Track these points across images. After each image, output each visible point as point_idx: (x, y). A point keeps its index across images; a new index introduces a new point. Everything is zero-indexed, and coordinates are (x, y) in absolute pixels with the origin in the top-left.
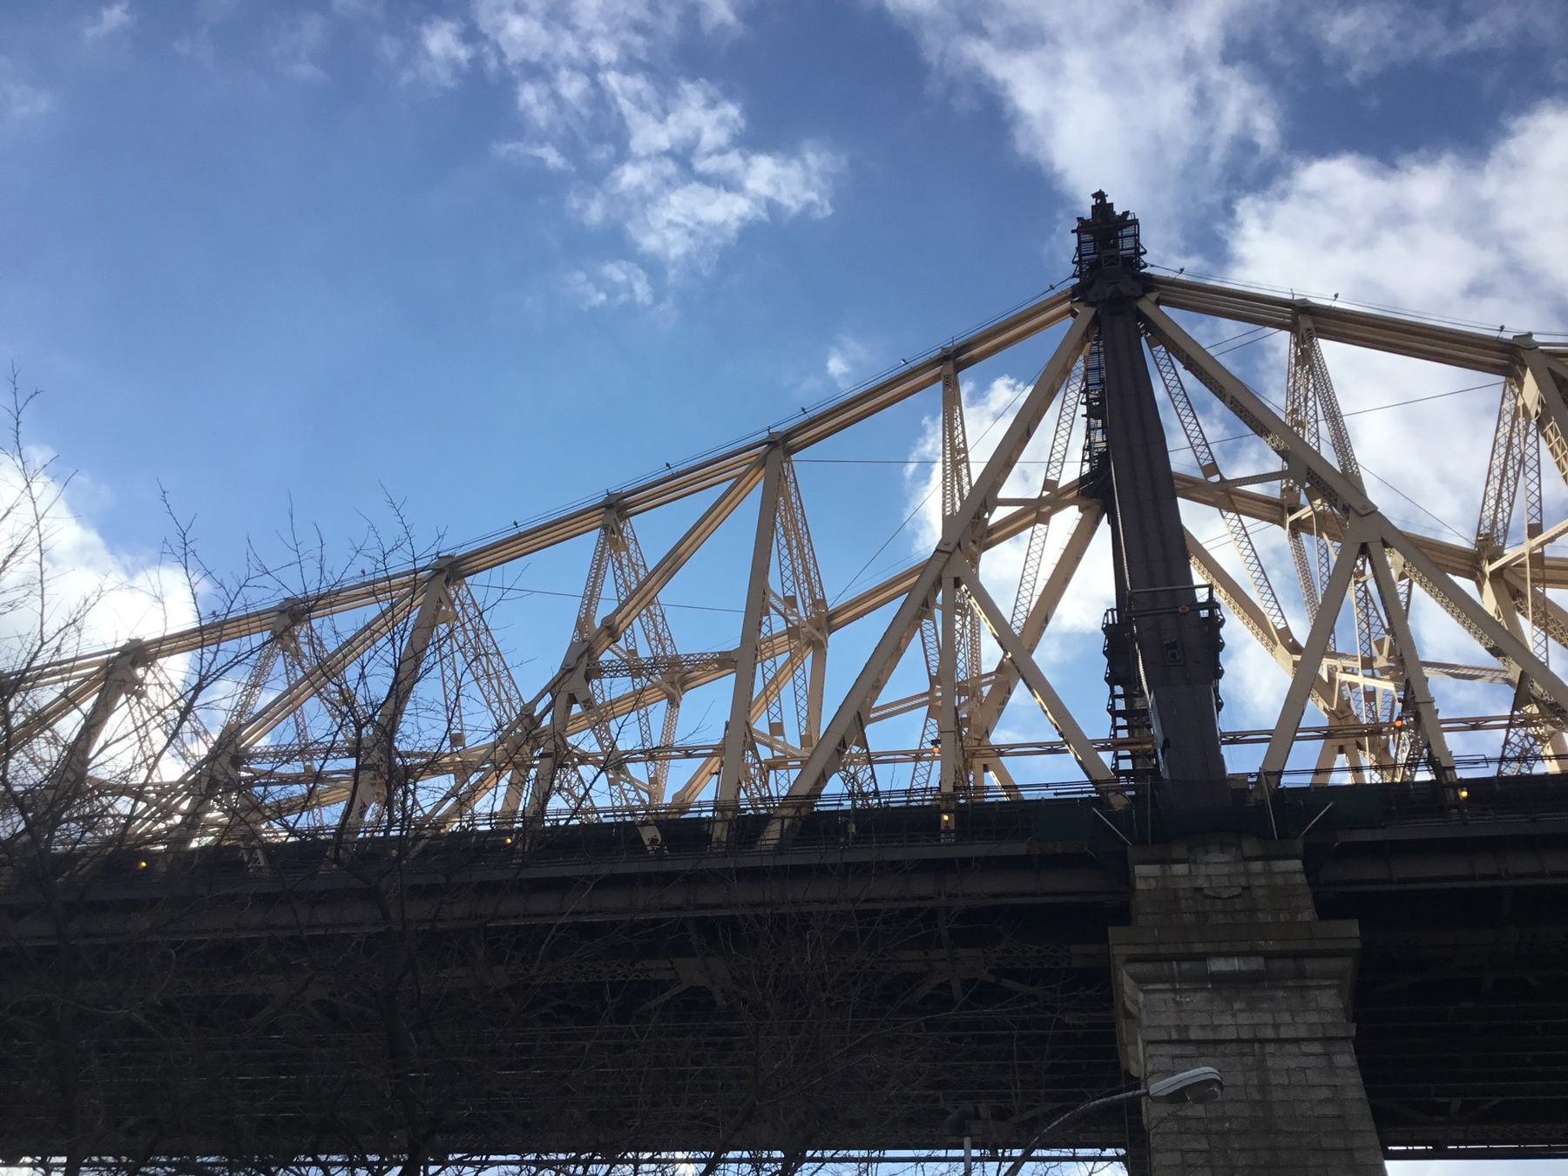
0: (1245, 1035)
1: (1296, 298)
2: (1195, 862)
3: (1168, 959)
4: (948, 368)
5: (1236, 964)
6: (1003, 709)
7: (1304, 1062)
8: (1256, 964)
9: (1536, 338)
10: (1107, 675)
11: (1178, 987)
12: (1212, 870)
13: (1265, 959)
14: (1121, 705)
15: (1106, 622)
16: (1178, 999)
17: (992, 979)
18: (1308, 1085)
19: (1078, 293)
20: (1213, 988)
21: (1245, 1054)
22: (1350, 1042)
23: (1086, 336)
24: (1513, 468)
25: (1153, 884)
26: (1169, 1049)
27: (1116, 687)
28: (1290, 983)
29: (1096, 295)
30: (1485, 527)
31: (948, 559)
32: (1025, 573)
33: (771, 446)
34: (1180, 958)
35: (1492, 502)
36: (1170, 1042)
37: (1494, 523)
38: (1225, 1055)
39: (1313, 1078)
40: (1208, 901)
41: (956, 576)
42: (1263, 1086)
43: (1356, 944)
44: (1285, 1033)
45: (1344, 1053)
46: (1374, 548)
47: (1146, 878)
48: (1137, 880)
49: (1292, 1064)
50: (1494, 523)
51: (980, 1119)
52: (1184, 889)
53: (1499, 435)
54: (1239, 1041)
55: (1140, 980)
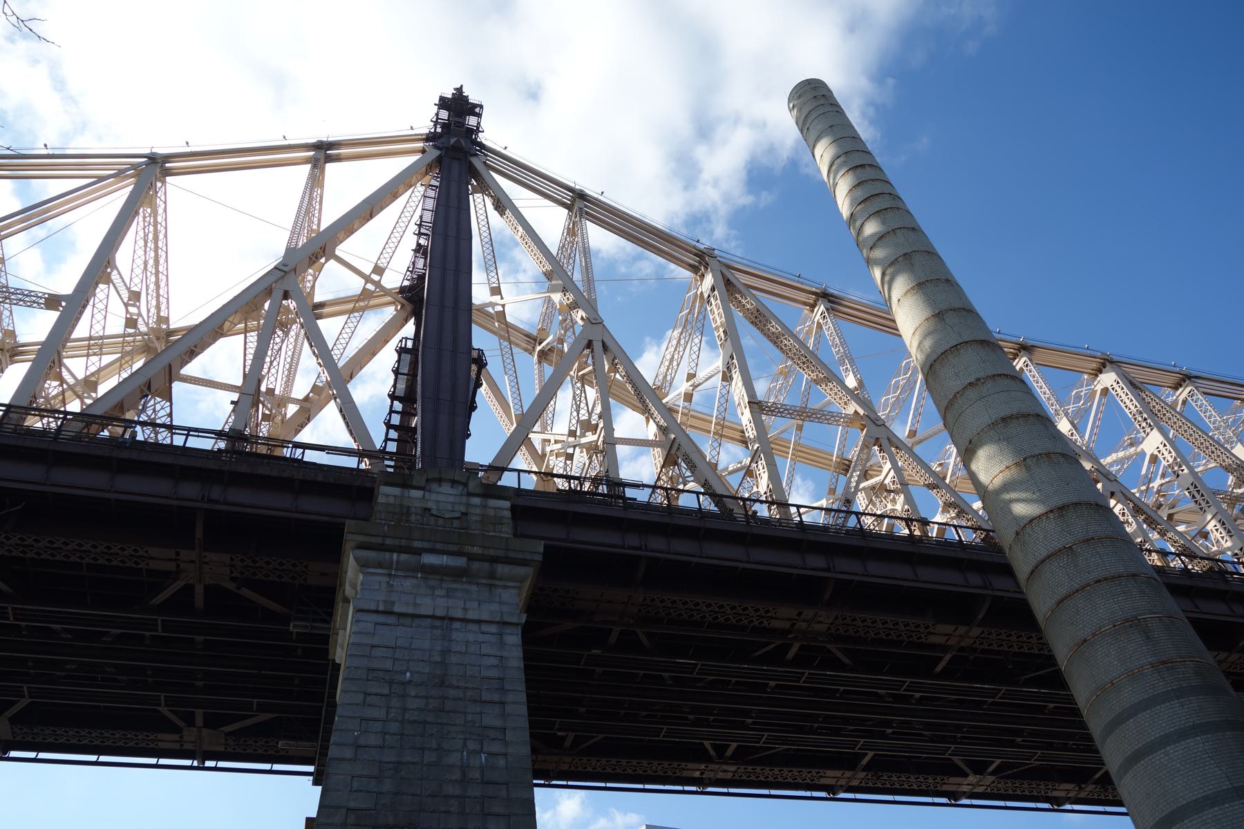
0: (440, 613)
1: (577, 187)
2: (430, 491)
3: (391, 550)
4: (321, 155)
5: (443, 560)
6: (300, 430)
7: (481, 638)
8: (460, 562)
9: (716, 252)
10: (390, 393)
11: (393, 573)
12: (441, 498)
13: (469, 559)
14: (396, 419)
15: (399, 346)
16: (391, 582)
17: (231, 586)
18: (481, 655)
19: (430, 138)
20: (421, 577)
21: (436, 628)
22: (519, 627)
23: (430, 168)
24: (685, 338)
25: (391, 500)
26: (374, 617)
27: (390, 430)
28: (484, 581)
29: (443, 143)
30: (659, 381)
31: (283, 277)
32: (341, 337)
33: (151, 161)
34: (400, 550)
35: (667, 363)
36: (377, 612)
37: (665, 377)
38: (419, 626)
39: (486, 649)
40: (432, 518)
41: (286, 289)
42: (445, 652)
43: (539, 558)
44: (472, 615)
45: (513, 634)
46: (598, 346)
47: (387, 496)
48: (380, 496)
49: (471, 638)
50: (665, 377)
51: (194, 726)
52: (416, 507)
53: (667, 352)
54: (433, 617)
55: (363, 565)
